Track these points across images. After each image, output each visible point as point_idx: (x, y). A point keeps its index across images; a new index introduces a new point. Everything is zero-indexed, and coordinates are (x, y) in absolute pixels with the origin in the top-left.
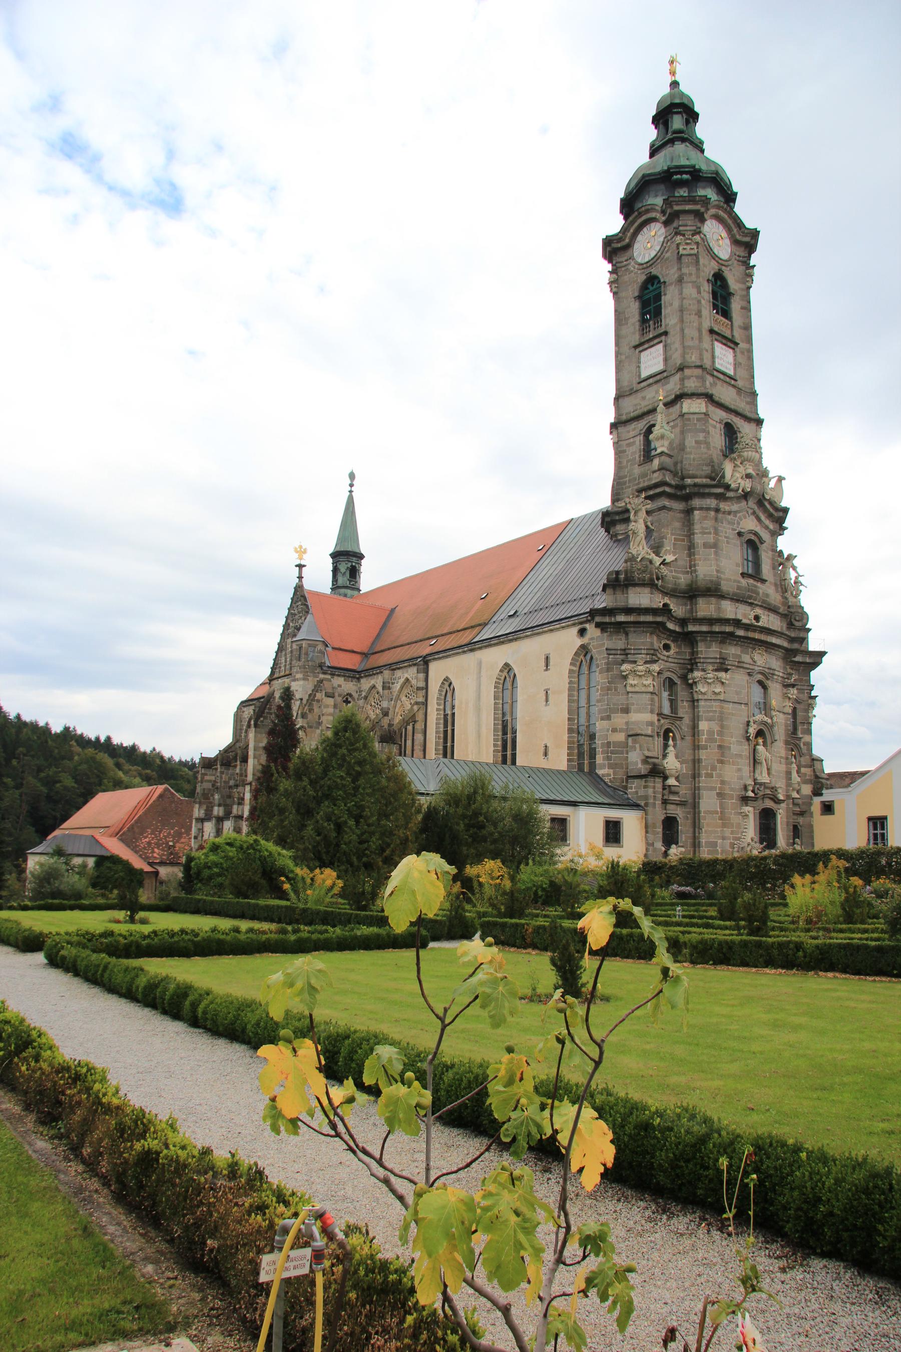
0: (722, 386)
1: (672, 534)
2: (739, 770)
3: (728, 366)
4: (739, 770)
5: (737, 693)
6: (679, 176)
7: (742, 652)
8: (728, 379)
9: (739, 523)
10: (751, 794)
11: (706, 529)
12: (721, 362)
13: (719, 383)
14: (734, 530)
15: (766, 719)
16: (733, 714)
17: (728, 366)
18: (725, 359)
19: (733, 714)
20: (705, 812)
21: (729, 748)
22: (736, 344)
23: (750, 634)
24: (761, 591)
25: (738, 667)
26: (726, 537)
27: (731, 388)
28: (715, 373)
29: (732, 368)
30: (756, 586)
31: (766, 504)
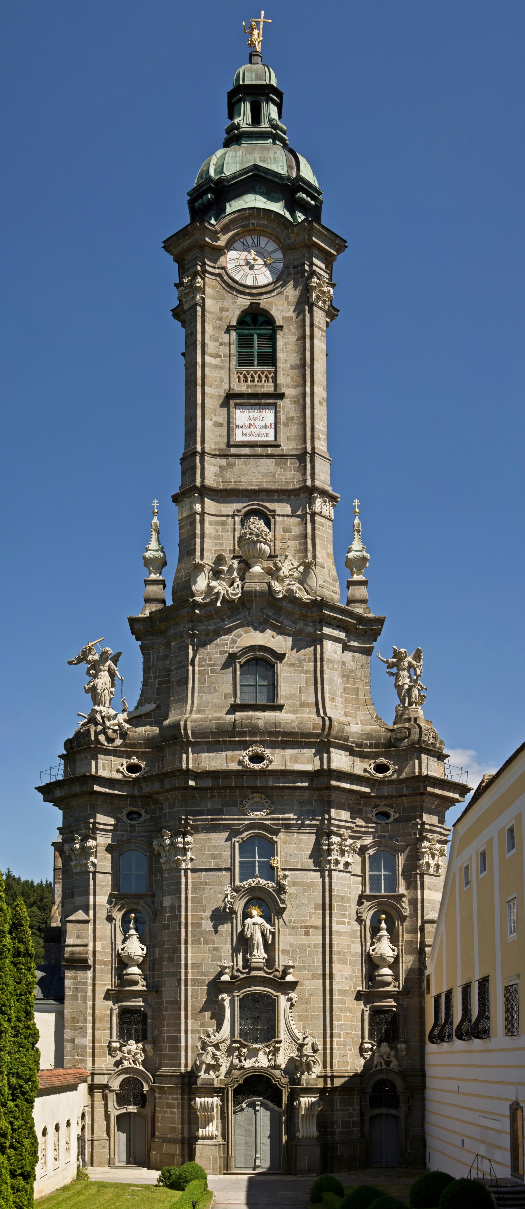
0: (245, 464)
1: (155, 677)
2: (217, 949)
3: (264, 431)
4: (217, 949)
5: (214, 857)
6: (200, 201)
7: (223, 805)
8: (259, 450)
9: (234, 642)
10: (226, 978)
11: (181, 662)
12: (247, 431)
13: (239, 462)
14: (223, 652)
15: (263, 882)
16: (206, 884)
17: (264, 431)
18: (257, 423)
19: (206, 884)
20: (167, 1002)
22: (281, 396)
23: (221, 783)
24: (261, 723)
26: (209, 665)
27: (264, 461)
28: (233, 451)
29: (271, 432)
30: (251, 718)
31: (284, 603)
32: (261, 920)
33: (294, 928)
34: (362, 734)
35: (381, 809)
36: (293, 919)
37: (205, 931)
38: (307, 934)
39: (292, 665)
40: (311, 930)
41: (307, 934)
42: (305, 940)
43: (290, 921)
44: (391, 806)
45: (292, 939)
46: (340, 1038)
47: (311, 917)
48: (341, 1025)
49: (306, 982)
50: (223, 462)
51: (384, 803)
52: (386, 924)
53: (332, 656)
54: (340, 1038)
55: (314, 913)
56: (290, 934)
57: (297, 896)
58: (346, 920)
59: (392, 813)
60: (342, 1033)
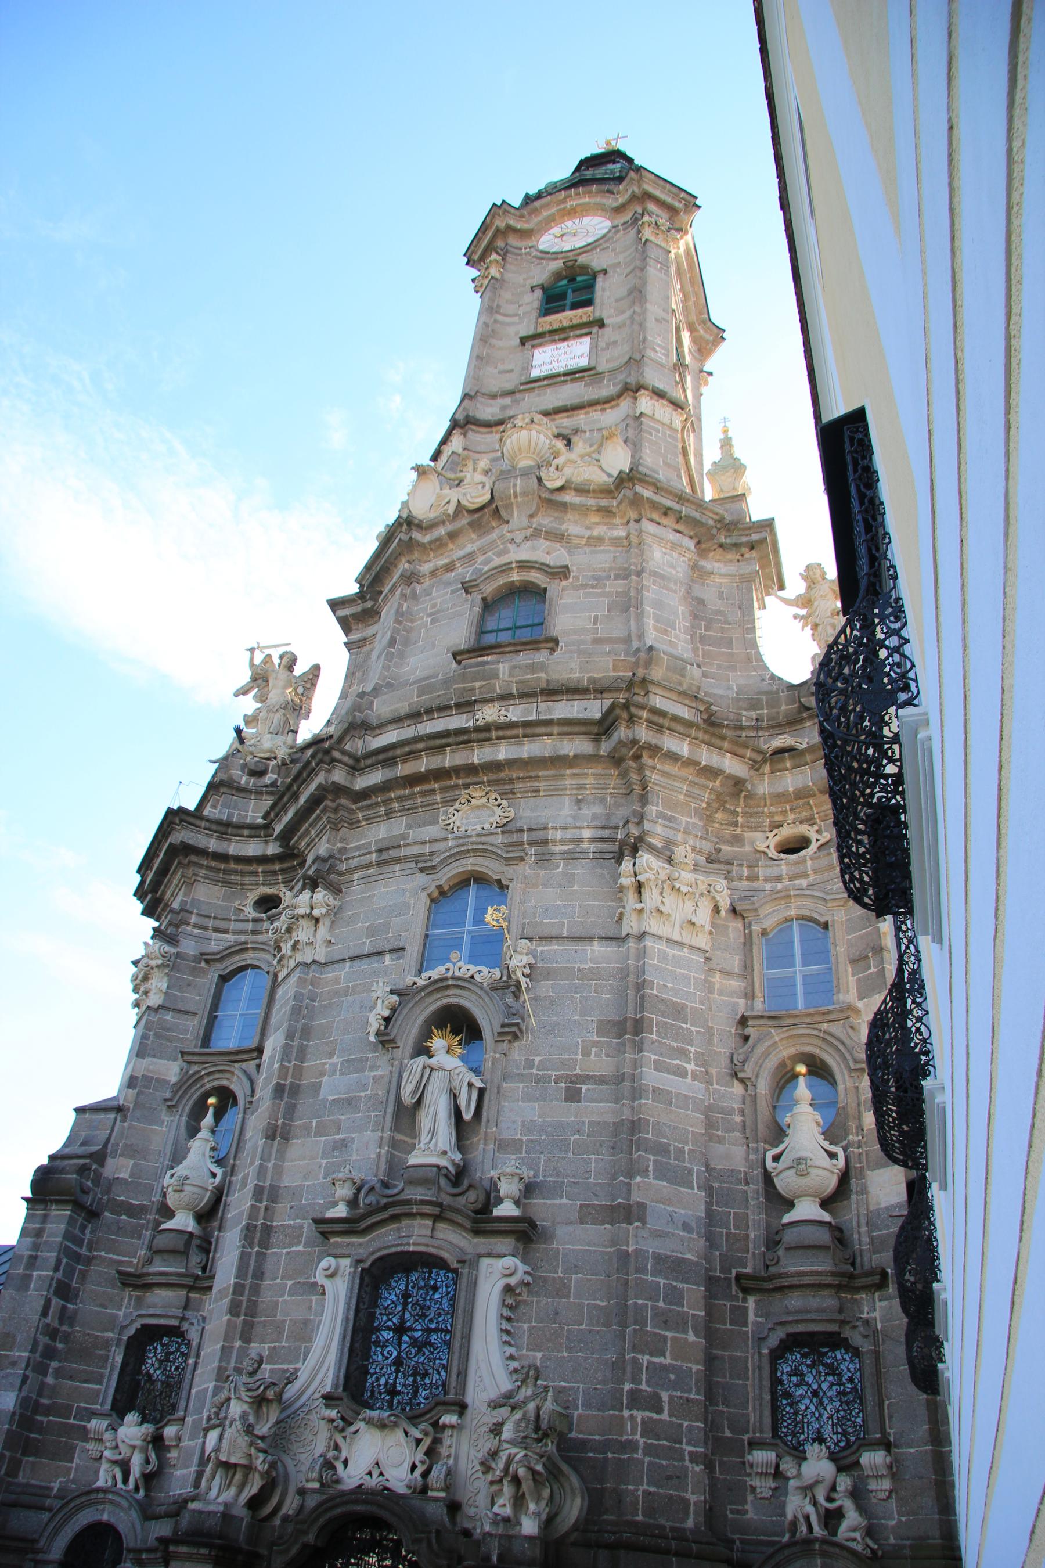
16: (346, 991)
19: (346, 991)
21: (316, 1088)
25: (379, 864)
32: (452, 1062)
33: (538, 1081)
34: (738, 700)
35: (787, 832)
36: (537, 1059)
37: (325, 1100)
38: (572, 1096)
39: (584, 586)
40: (584, 1087)
41: (572, 1096)
42: (567, 1113)
43: (530, 1064)
44: (810, 821)
45: (532, 1111)
46: (660, 1411)
47: (586, 1053)
48: (664, 1368)
49: (561, 1231)
50: (507, 401)
51: (791, 817)
52: (810, 1087)
53: (663, 570)
54: (660, 1411)
55: (595, 1044)
56: (527, 1098)
57: (552, 1003)
58: (690, 1067)
59: (813, 836)
60: (665, 1396)
